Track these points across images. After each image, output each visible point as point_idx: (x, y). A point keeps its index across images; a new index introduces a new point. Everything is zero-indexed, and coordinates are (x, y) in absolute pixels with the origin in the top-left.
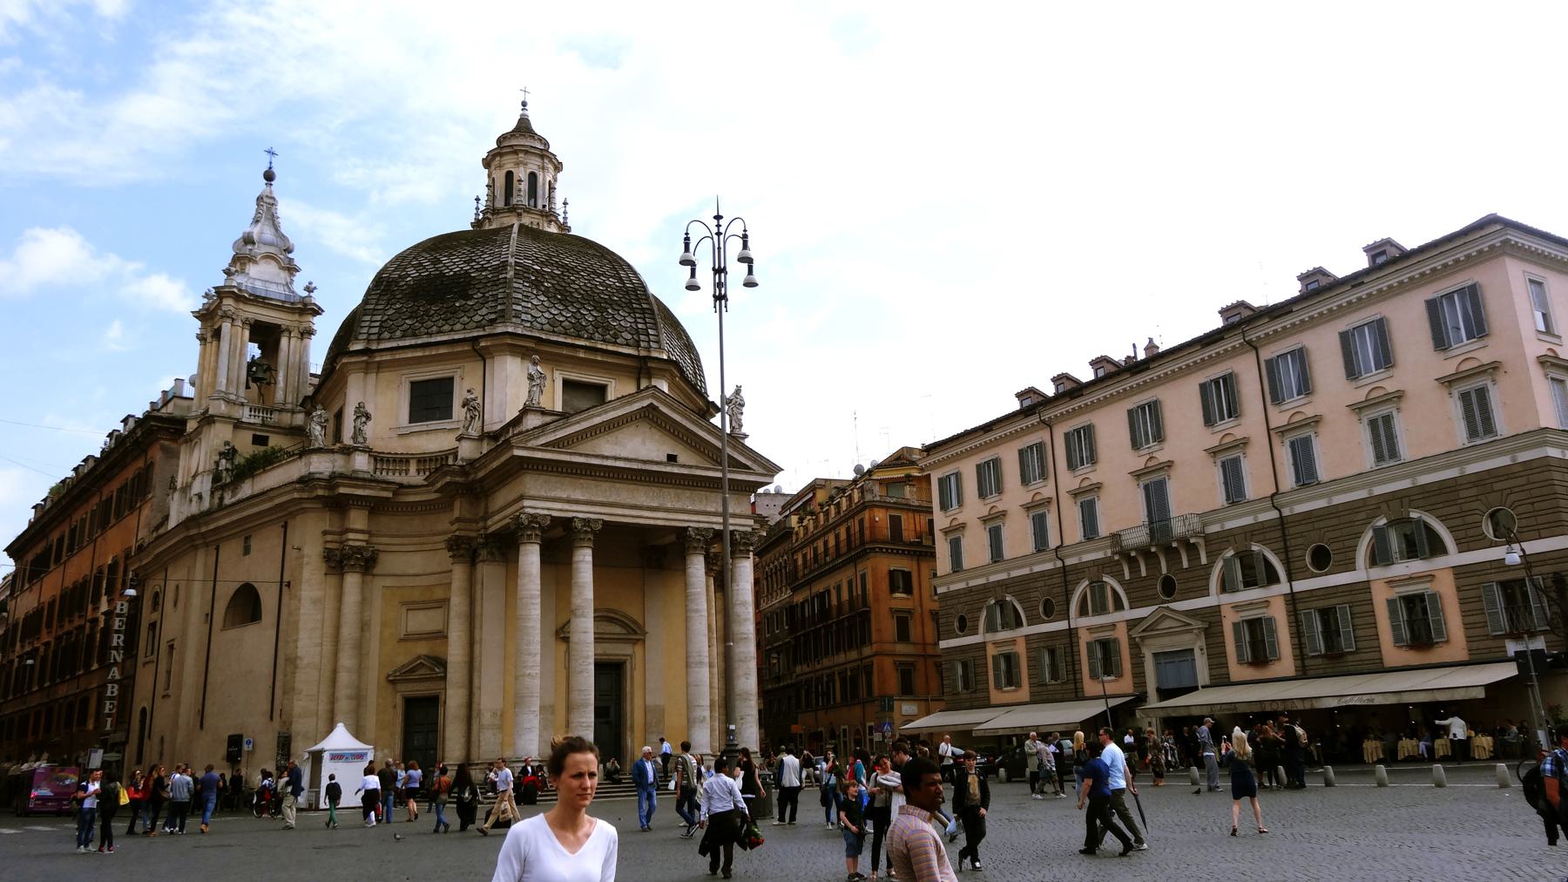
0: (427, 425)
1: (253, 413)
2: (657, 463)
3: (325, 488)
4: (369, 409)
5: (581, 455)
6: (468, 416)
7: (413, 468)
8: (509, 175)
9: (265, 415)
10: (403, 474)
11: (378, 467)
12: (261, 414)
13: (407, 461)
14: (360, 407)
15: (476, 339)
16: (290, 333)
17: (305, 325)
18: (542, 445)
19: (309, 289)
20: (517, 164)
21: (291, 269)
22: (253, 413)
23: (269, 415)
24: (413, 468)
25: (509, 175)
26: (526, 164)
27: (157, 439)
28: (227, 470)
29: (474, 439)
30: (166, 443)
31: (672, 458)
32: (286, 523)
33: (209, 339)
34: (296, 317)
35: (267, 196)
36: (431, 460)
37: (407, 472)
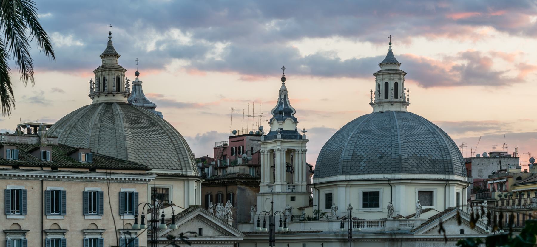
0: (370, 209)
1: (289, 188)
2: (458, 235)
3: (341, 236)
4: (352, 206)
5: (434, 235)
6: (390, 212)
7: (366, 224)
8: (387, 84)
9: (293, 188)
10: (362, 227)
11: (354, 225)
12: (292, 188)
13: (364, 222)
14: (349, 205)
15: (389, 180)
16: (298, 152)
17: (303, 148)
18: (422, 234)
19: (304, 132)
20: (390, 79)
21: (295, 121)
22: (289, 188)
23: (294, 188)
24: (366, 224)
25: (387, 84)
26: (393, 79)
27: (237, 185)
28: (289, 215)
29: (392, 221)
30: (239, 186)
31: (462, 231)
32: (323, 244)
33: (266, 153)
34: (300, 145)
35: (285, 90)
36: (372, 222)
37: (364, 226)
